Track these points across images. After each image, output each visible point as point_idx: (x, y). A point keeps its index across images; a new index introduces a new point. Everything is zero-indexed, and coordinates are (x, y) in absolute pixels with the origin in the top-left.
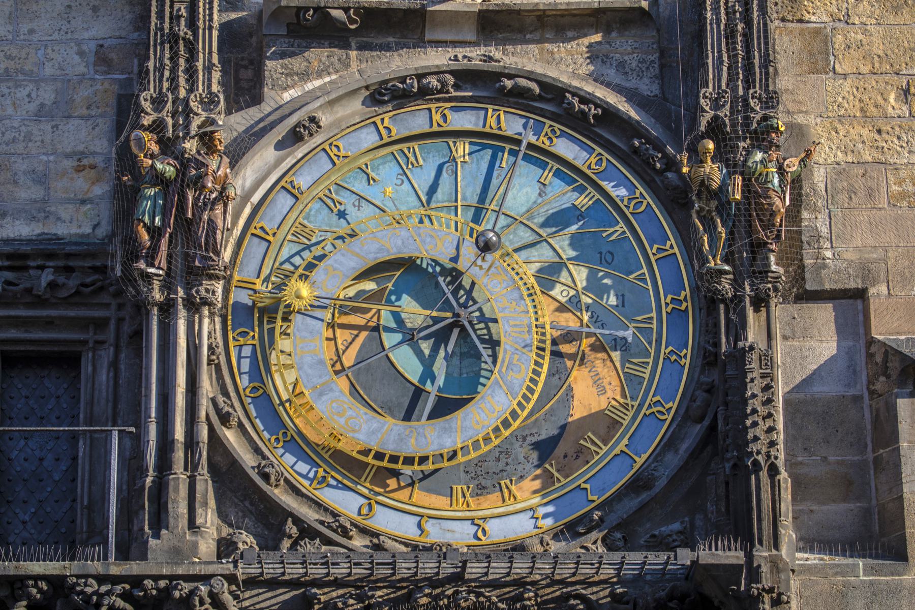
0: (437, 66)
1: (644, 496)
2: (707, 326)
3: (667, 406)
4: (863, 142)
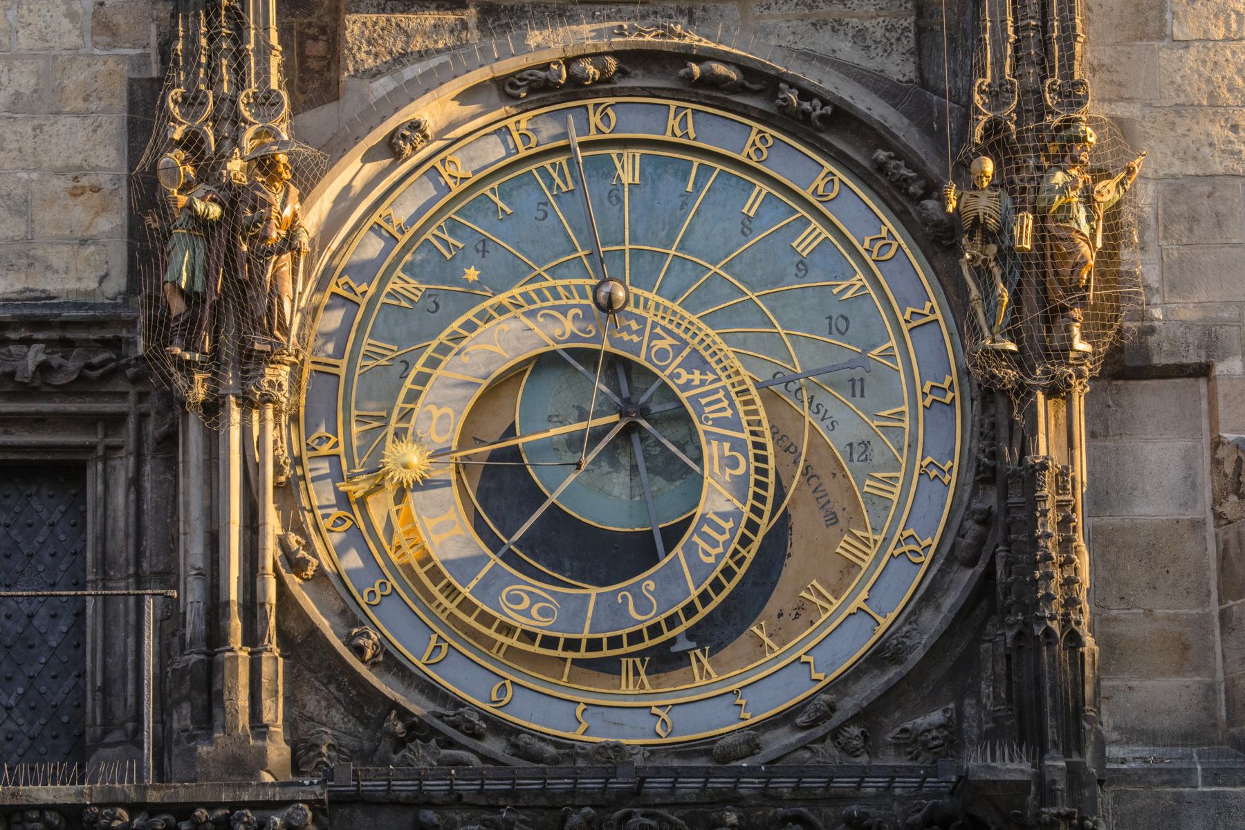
1: (892, 673)
2: (982, 426)
3: (924, 544)
4: (1211, 145)
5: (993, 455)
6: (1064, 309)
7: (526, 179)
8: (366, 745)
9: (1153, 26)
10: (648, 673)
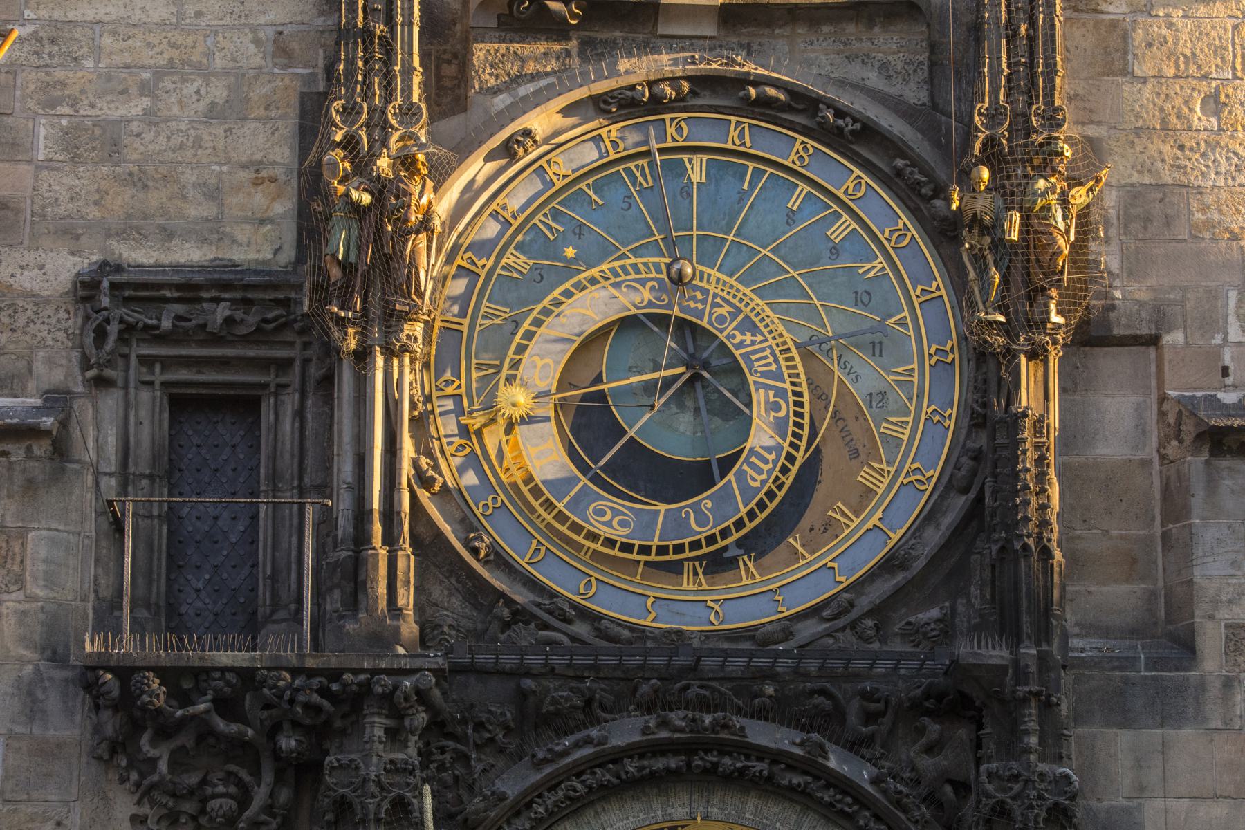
1: (900, 577)
3: (928, 475)
4: (1163, 160)
6: (1043, 289)
7: (615, 177)
8: (480, 626)
9: (1118, 64)
10: (704, 574)
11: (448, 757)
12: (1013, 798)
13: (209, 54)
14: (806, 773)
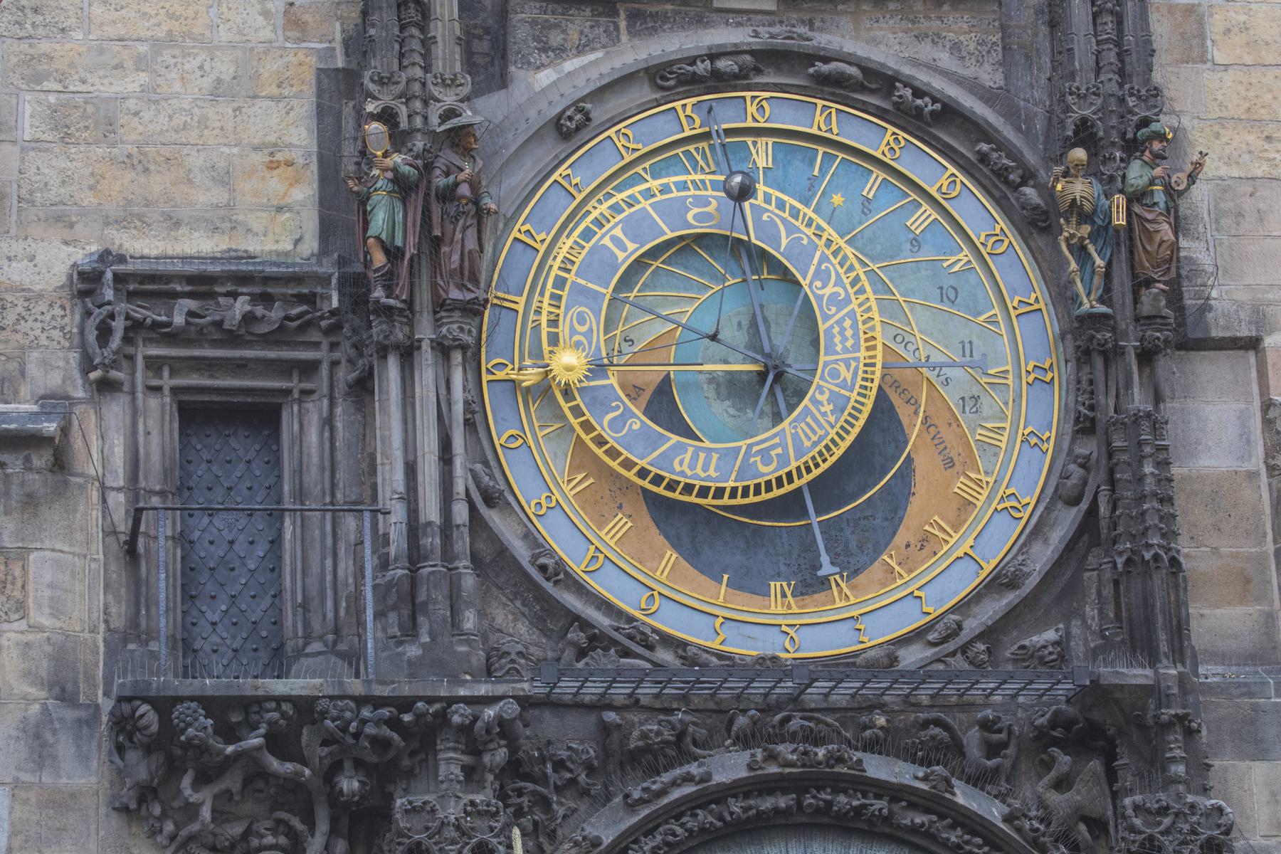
0: (735, 45)
1: (1010, 598)
2: (1079, 382)
5: (1092, 408)
8: (550, 654)
9: (1196, 52)
10: (793, 595)
11: (525, 800)
12: (1162, 833)
13: (214, 27)
14: (928, 811)
